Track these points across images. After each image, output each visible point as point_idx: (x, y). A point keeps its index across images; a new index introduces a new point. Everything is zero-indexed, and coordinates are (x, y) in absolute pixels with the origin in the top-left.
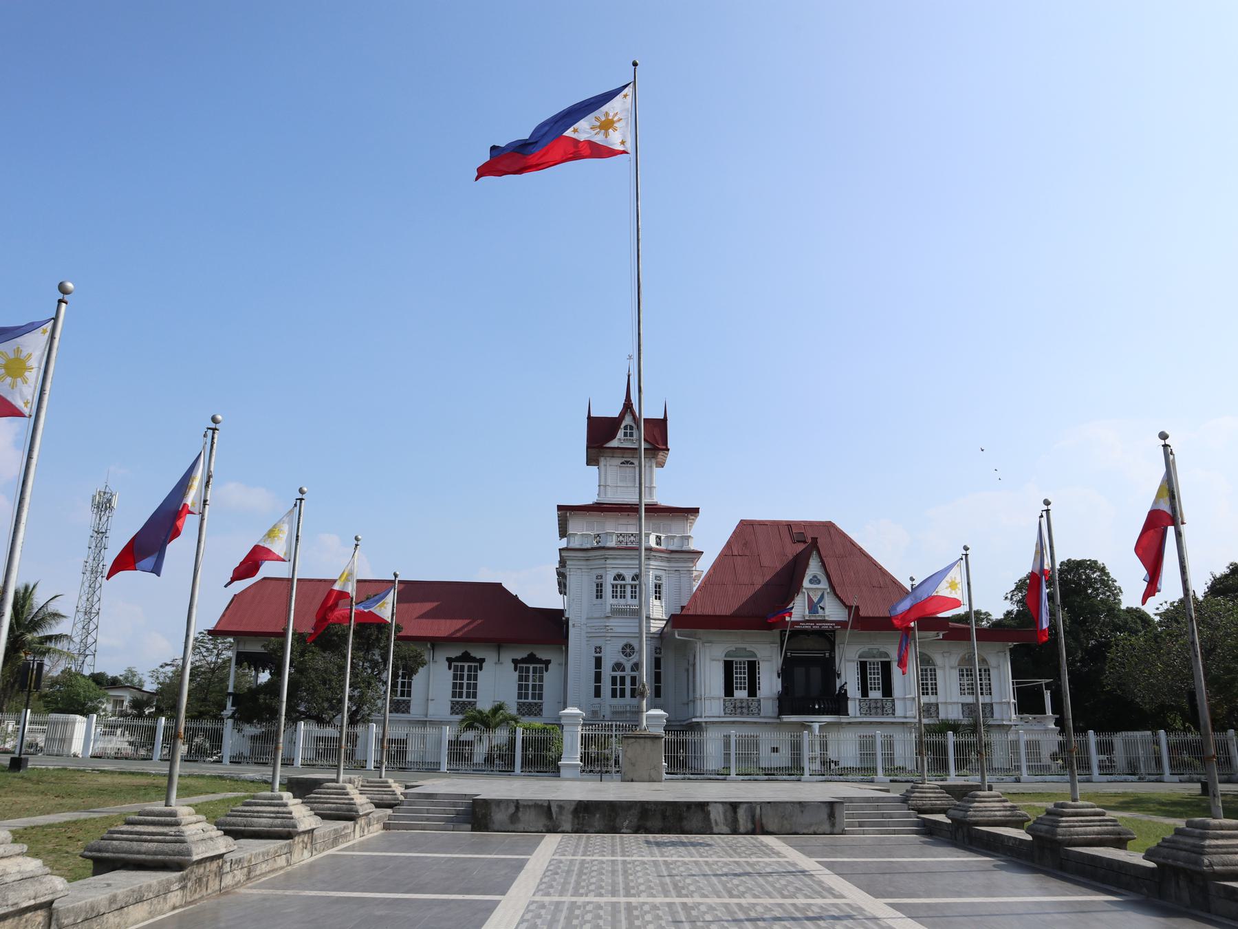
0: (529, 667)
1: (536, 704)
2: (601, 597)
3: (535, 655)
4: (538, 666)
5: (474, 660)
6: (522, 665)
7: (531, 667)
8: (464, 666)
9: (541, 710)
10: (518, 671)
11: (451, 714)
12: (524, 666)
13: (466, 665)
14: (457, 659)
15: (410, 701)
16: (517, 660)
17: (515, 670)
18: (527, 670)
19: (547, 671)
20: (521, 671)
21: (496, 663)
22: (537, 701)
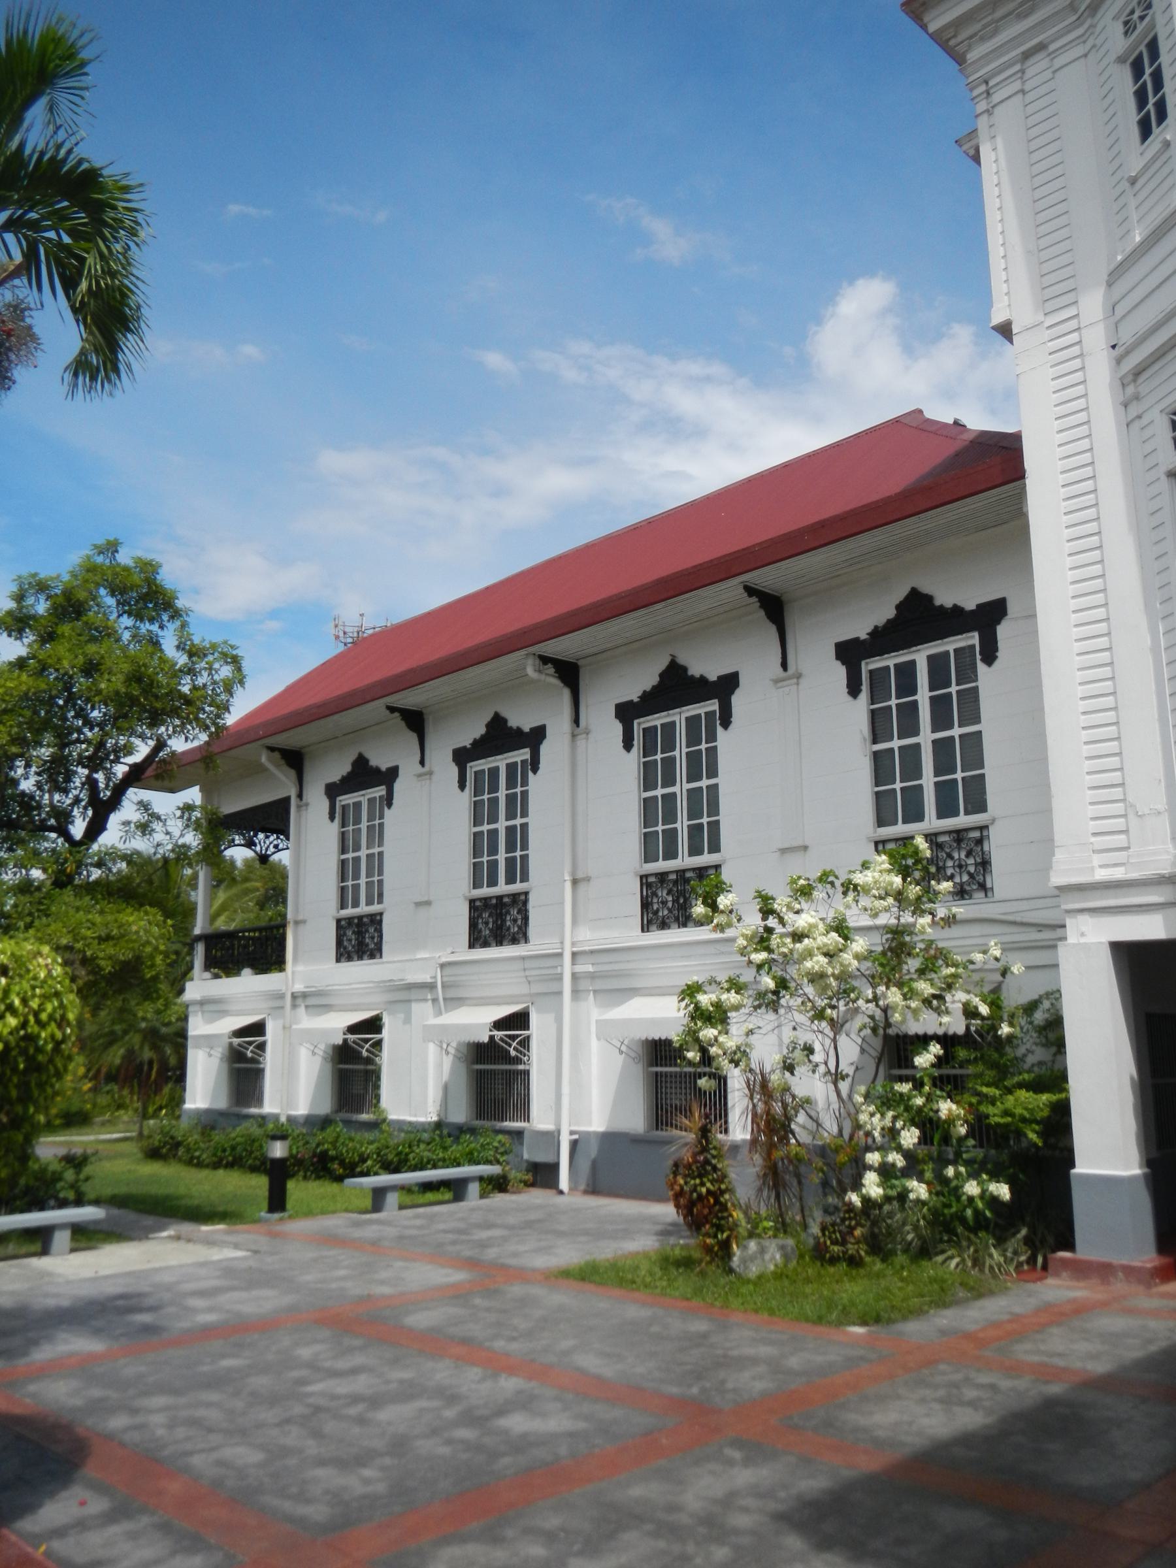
0: (913, 663)
1: (959, 835)
2: (1162, 115)
3: (929, 599)
4: (950, 645)
5: (700, 689)
6: (876, 663)
7: (920, 656)
8: (673, 724)
9: (985, 864)
10: (864, 696)
11: (645, 928)
12: (890, 661)
13: (679, 717)
14: (652, 702)
15: (526, 894)
16: (856, 641)
17: (854, 690)
18: (907, 672)
19: (990, 654)
20: (878, 689)
21: (776, 681)
22: (962, 820)
